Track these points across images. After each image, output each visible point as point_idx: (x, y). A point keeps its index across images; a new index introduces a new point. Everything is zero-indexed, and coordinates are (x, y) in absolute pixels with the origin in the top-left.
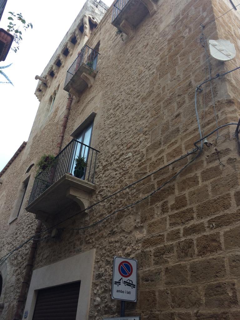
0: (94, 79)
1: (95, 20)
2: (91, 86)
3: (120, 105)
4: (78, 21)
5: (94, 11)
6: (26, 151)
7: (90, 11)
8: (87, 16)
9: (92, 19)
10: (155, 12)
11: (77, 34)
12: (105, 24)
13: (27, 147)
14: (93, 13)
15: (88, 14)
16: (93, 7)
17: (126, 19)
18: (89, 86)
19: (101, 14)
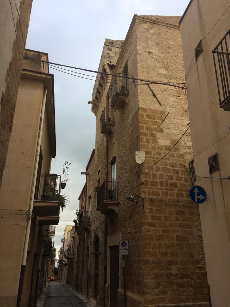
0: (114, 127)
1: (112, 63)
2: (113, 133)
3: (122, 158)
4: (102, 68)
6: (96, 156)
13: (96, 152)
15: (106, 62)
18: (112, 132)
19: (115, 55)
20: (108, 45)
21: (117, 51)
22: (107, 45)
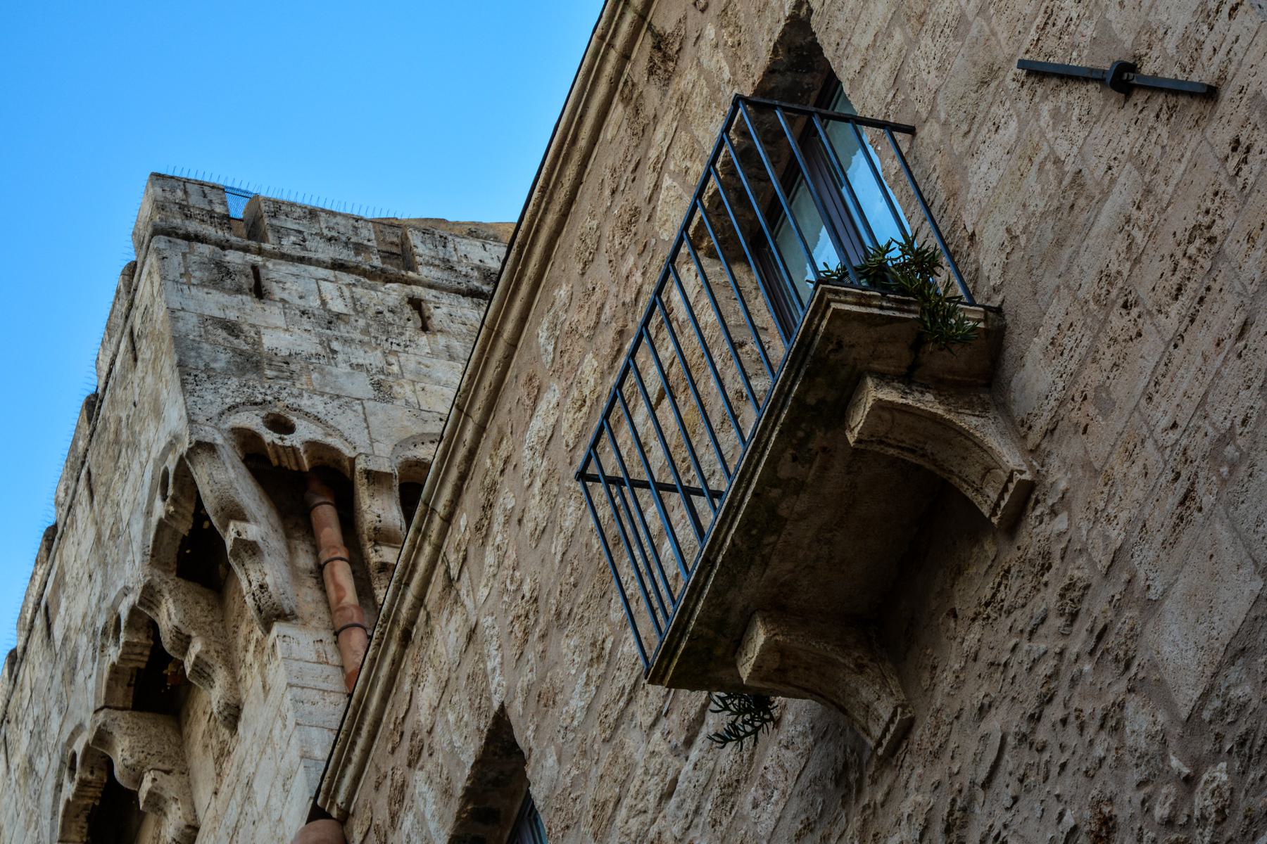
1: (305, 432)
5: (257, 343)
7: (226, 373)
8: (219, 440)
9: (269, 437)
10: (1026, 495)
11: (178, 631)
12: (482, 529)
14: (252, 378)
16: (232, 315)
17: (776, 607)
19: (325, 343)
20: (198, 238)
21: (337, 306)
22: (198, 238)
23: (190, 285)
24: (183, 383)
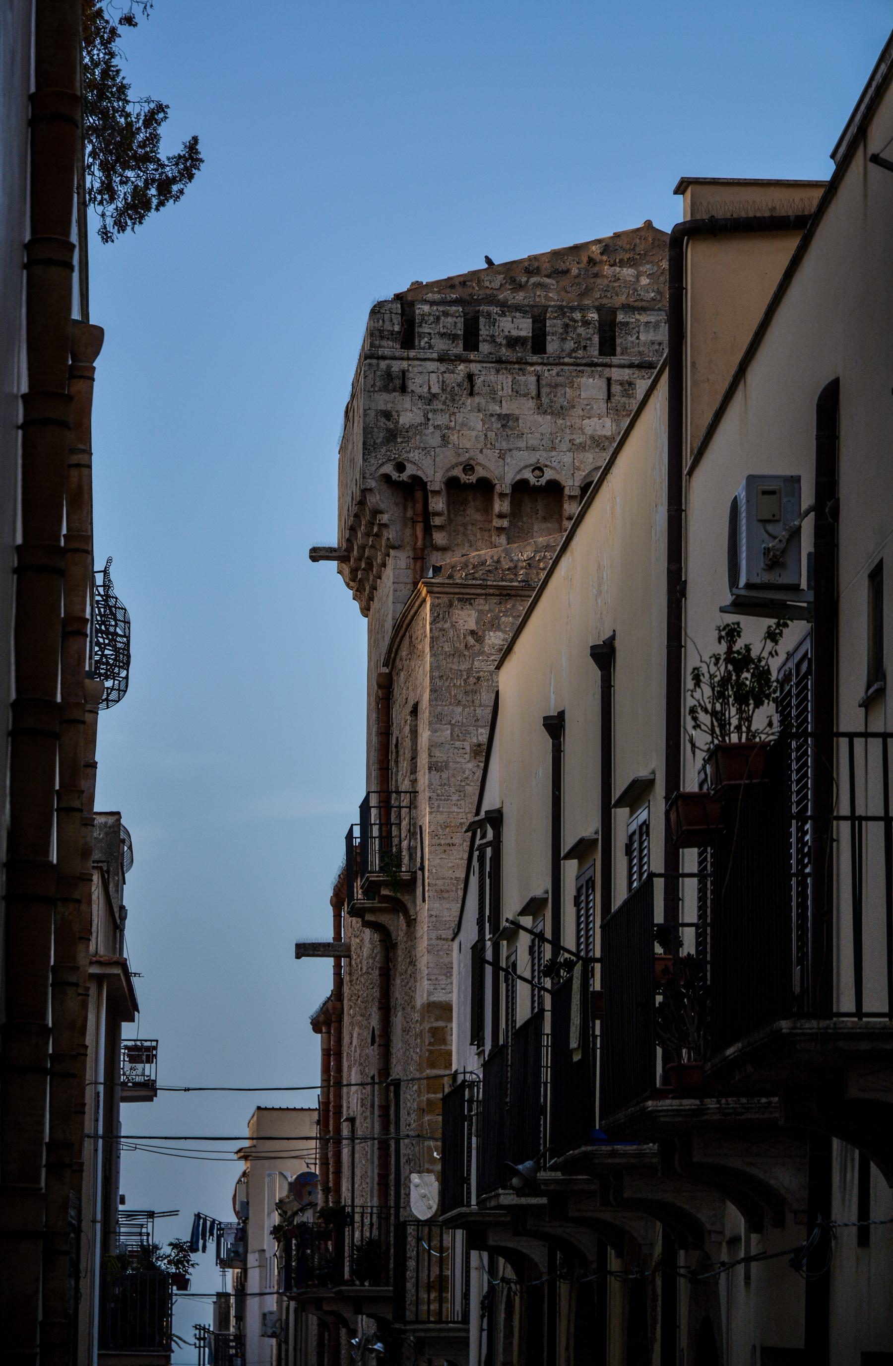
1: (410, 470)
21: (435, 389)
23: (374, 391)
24: (364, 454)
